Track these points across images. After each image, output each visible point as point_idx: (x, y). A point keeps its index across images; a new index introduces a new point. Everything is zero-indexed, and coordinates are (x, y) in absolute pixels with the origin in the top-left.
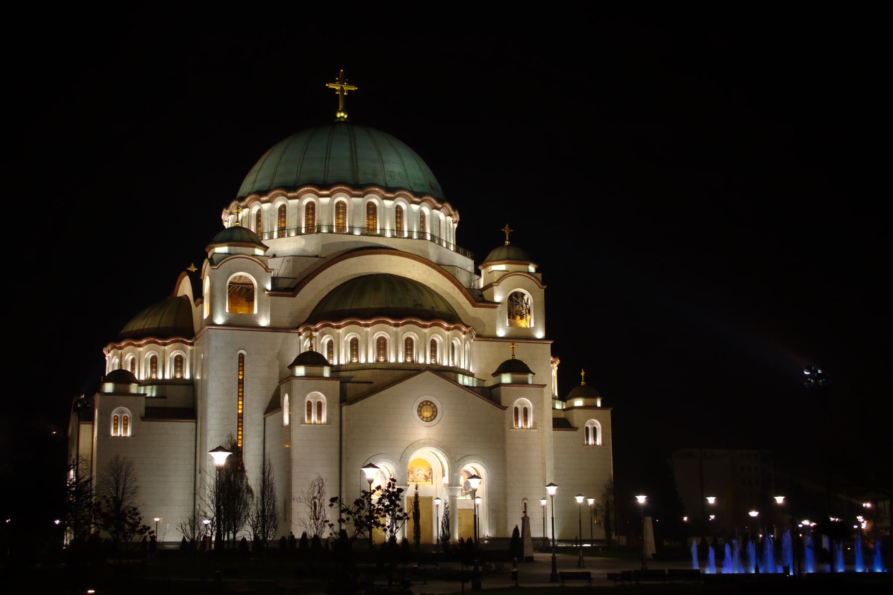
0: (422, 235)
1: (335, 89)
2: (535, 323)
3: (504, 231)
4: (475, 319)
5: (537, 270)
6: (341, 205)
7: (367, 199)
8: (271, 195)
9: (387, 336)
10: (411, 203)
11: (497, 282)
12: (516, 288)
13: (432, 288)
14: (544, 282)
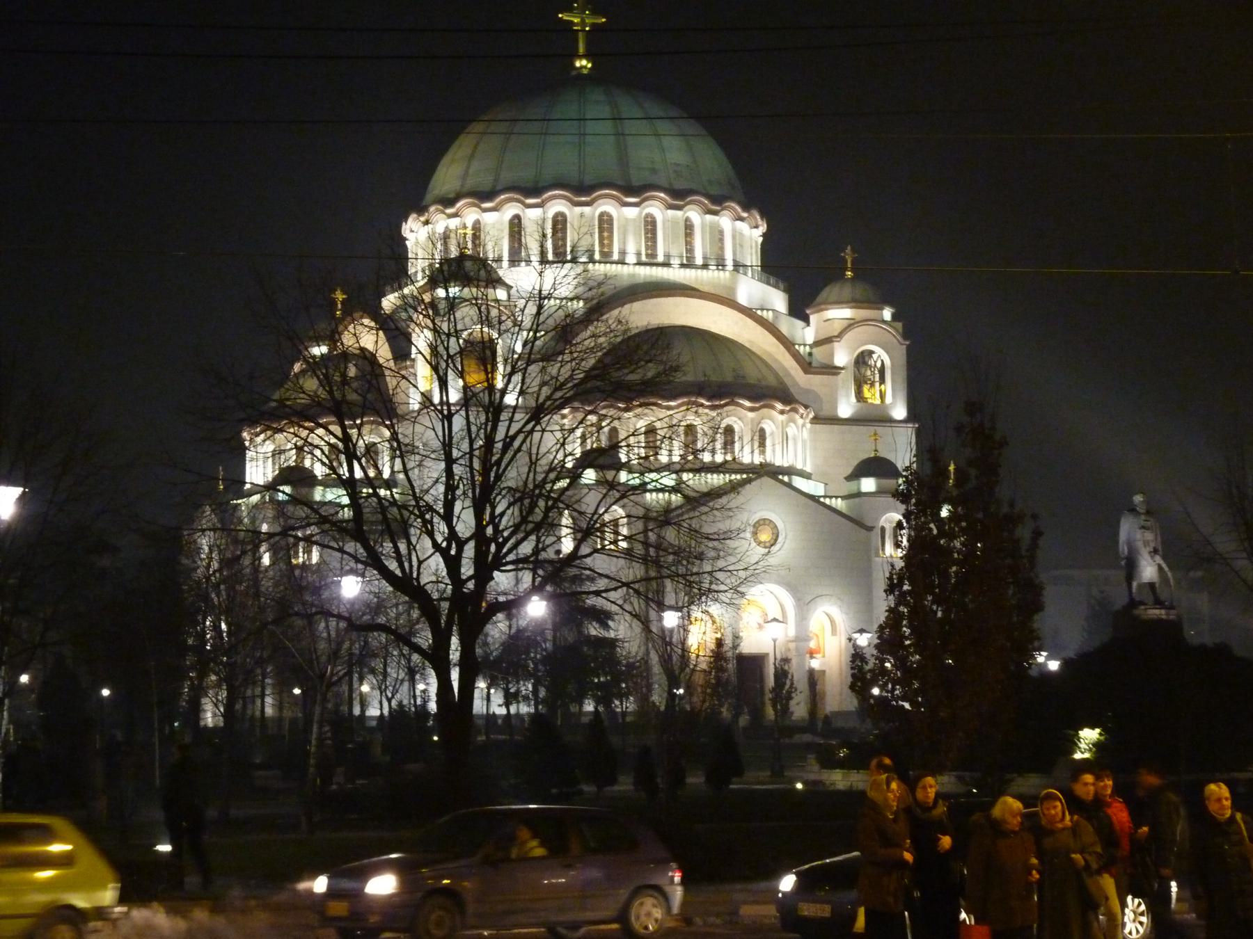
0: (721, 264)
1: (572, 22)
2: (894, 396)
3: (844, 257)
4: (808, 391)
5: (895, 317)
6: (605, 218)
7: (644, 208)
8: (498, 200)
9: (697, 422)
10: (706, 213)
11: (838, 336)
12: (866, 344)
13: (747, 345)
14: (905, 335)
